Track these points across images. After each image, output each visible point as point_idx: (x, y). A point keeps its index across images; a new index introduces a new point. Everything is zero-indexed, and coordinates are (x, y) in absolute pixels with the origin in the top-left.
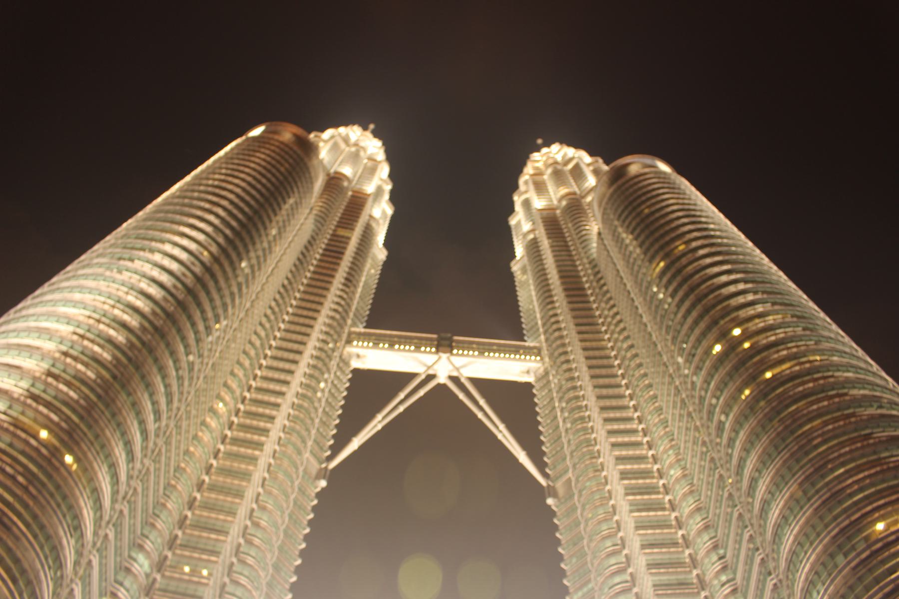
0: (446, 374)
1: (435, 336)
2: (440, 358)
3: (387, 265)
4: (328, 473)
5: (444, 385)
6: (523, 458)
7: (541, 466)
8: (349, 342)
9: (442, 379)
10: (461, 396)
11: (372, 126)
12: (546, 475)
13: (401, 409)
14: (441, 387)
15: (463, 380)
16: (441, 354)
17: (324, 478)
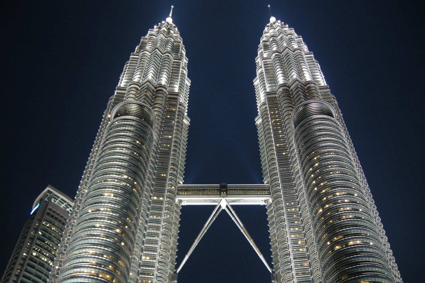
0: (226, 206)
1: (219, 185)
2: (221, 200)
3: (191, 128)
4: (177, 275)
5: (224, 210)
6: (261, 257)
7: (269, 261)
8: (178, 194)
9: (224, 207)
10: (233, 219)
11: (172, 7)
12: (271, 266)
13: (206, 231)
14: (224, 211)
15: (233, 212)
16: (221, 198)
17: (176, 280)
